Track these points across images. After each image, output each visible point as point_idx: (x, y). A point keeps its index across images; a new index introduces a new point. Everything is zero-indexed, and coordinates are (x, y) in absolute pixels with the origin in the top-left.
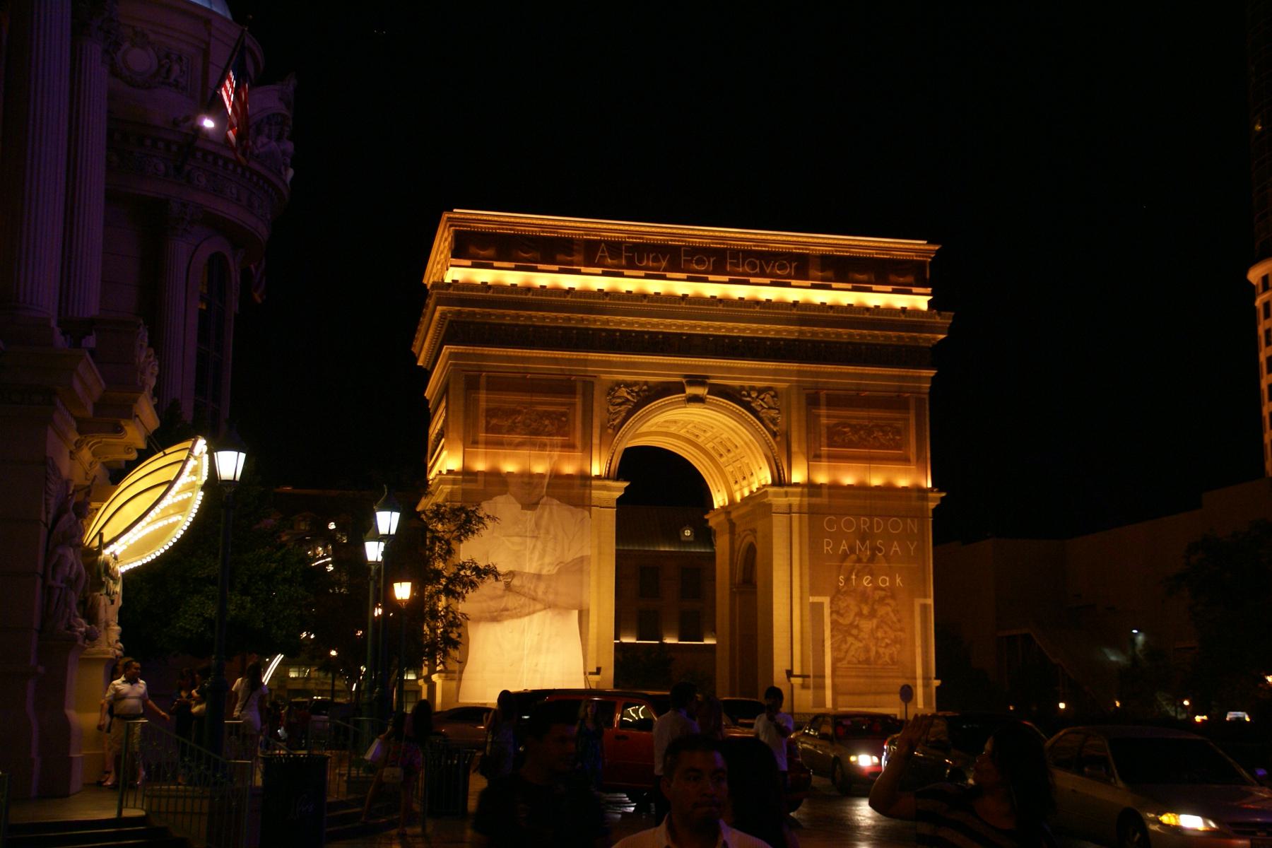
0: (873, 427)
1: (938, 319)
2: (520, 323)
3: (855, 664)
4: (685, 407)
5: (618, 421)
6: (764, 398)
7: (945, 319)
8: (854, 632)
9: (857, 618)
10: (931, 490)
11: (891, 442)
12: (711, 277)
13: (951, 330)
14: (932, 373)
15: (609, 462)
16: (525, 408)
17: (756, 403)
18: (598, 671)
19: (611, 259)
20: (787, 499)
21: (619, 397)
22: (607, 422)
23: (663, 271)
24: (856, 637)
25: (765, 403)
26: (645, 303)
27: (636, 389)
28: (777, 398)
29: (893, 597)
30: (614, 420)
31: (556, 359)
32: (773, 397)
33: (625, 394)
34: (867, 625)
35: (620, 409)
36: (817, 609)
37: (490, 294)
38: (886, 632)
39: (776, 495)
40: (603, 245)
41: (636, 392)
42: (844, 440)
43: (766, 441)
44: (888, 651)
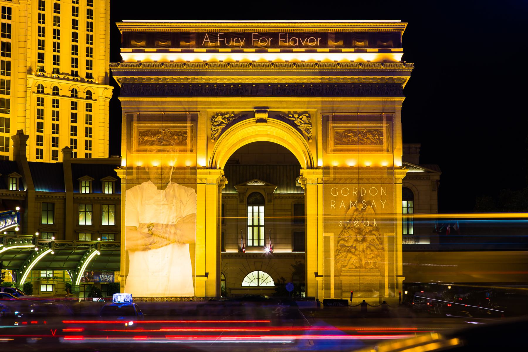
0: (367, 132)
1: (404, 67)
2: (159, 82)
3: (354, 269)
4: (256, 125)
5: (217, 135)
6: (302, 118)
7: (410, 67)
9: (355, 243)
10: (401, 168)
11: (378, 141)
12: (171, 50)
13: (413, 74)
14: (403, 99)
15: (212, 158)
17: (297, 121)
18: (207, 275)
19: (211, 42)
20: (314, 176)
22: (211, 136)
23: (242, 48)
24: (353, 254)
26: (229, 67)
27: (227, 116)
28: (310, 118)
30: (214, 134)
31: (154, 102)
32: (307, 117)
33: (221, 120)
34: (361, 246)
35: (218, 128)
36: (327, 240)
37: (141, 67)
38: (372, 250)
39: (308, 174)
40: (207, 34)
41: (227, 118)
42: (349, 140)
43: (303, 142)
44: (372, 261)
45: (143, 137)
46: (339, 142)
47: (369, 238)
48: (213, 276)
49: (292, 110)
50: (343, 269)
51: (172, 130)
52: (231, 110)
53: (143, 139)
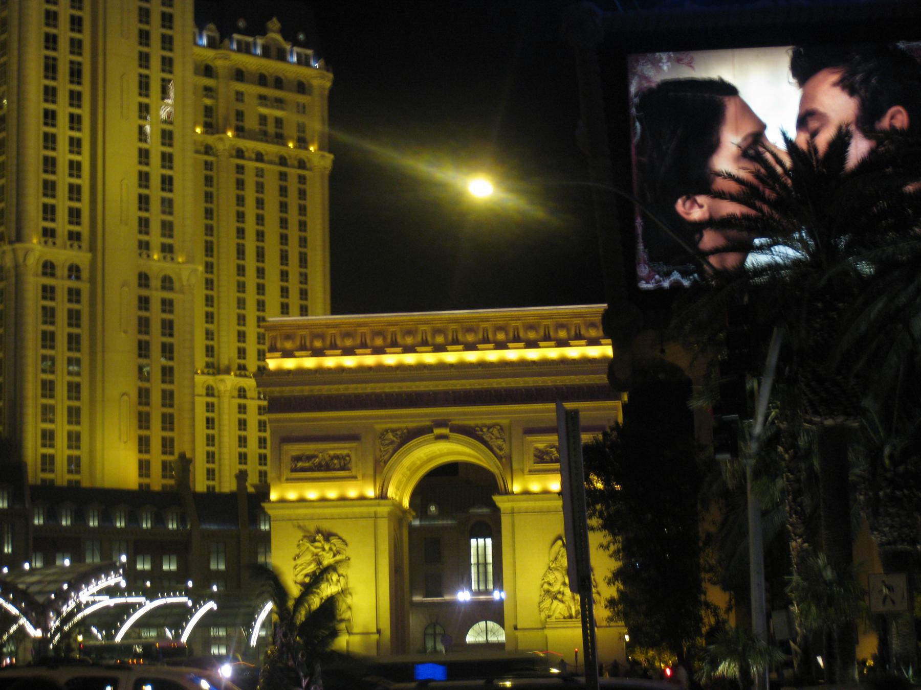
8: (559, 596)
16: (321, 453)
18: (379, 632)
21: (387, 439)
24: (562, 601)
25: (493, 434)
27: (399, 433)
30: (384, 456)
32: (498, 430)
45: (296, 462)
46: (538, 460)
48: (387, 633)
49: (479, 422)
50: (548, 620)
51: (332, 453)
52: (403, 425)
53: (296, 466)
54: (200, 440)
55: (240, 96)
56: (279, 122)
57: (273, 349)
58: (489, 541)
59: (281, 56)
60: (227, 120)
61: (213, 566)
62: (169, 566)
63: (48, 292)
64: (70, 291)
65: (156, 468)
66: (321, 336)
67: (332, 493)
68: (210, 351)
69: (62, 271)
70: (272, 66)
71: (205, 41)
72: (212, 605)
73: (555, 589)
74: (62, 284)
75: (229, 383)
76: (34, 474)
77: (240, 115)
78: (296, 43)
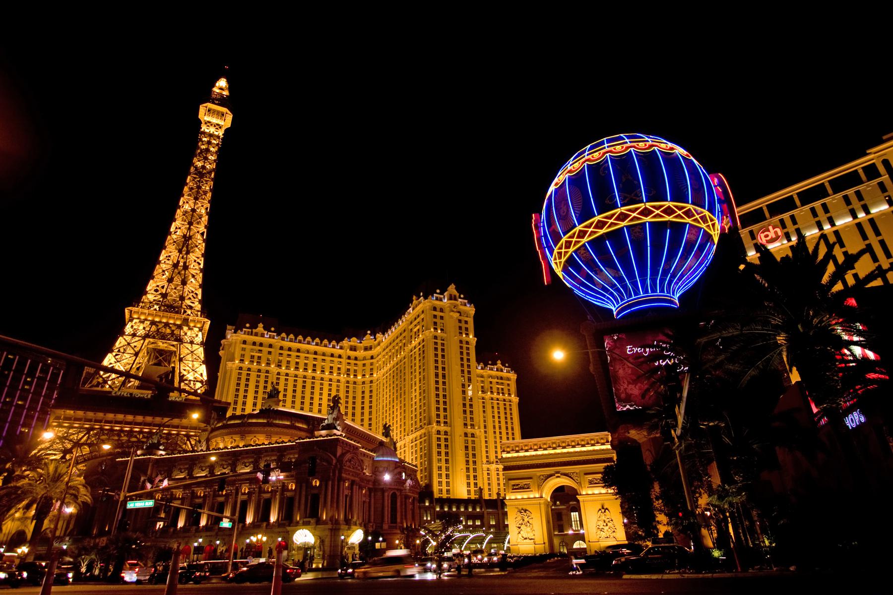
18: (544, 543)
29: (612, 520)
47: (609, 524)
48: (547, 544)
54: (486, 482)
55: (491, 382)
56: (502, 389)
57: (504, 451)
58: (577, 513)
59: (502, 371)
60: (488, 389)
61: (491, 523)
62: (478, 523)
63: (439, 439)
64: (445, 439)
65: (472, 492)
66: (518, 446)
67: (525, 497)
68: (487, 457)
69: (442, 433)
70: (500, 374)
71: (480, 368)
72: (491, 536)
73: (601, 527)
74: (443, 437)
75: (493, 467)
76: (436, 495)
77: (491, 388)
78: (506, 367)
